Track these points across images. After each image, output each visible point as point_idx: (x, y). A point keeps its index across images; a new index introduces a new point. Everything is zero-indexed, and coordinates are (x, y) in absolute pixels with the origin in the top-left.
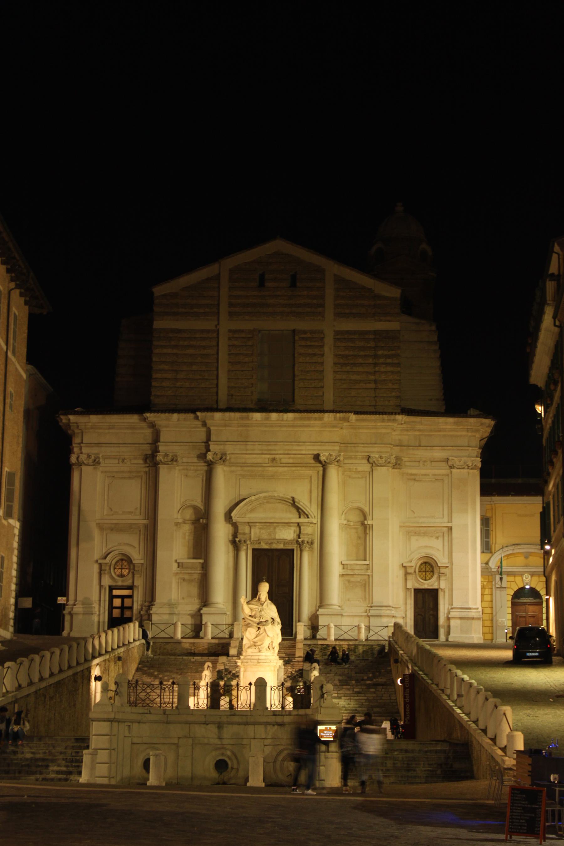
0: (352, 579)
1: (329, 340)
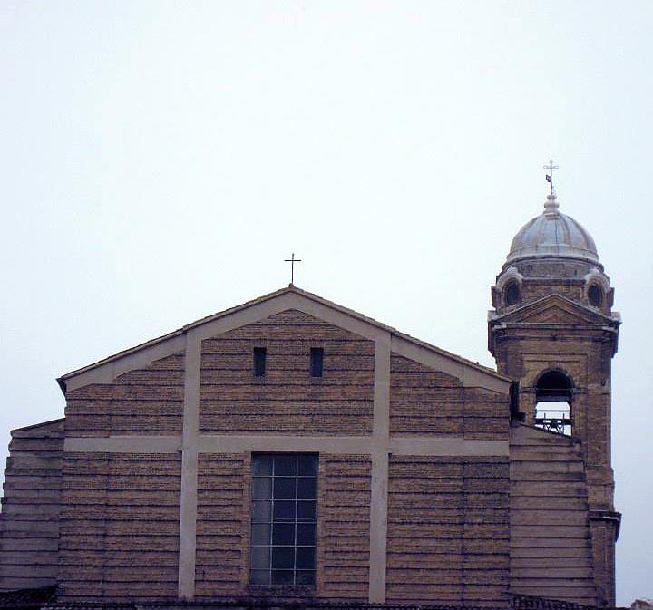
1: (380, 473)
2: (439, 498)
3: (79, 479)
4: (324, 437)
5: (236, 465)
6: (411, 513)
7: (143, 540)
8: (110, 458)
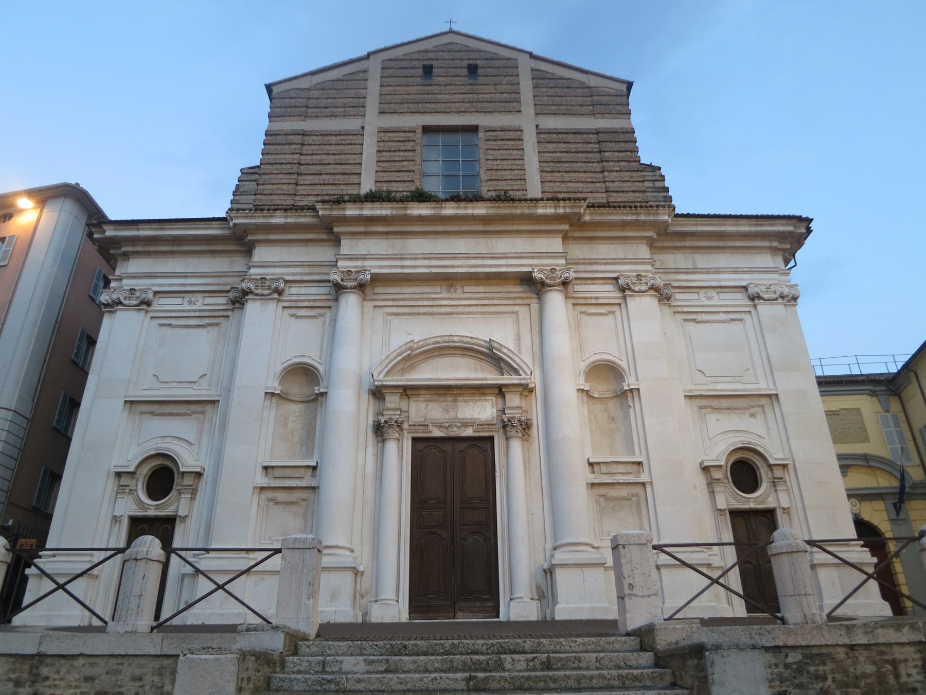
0: (612, 492)
2: (580, 155)
3: (278, 147)
4: (481, 116)
6: (559, 165)
7: (330, 187)
8: (304, 134)
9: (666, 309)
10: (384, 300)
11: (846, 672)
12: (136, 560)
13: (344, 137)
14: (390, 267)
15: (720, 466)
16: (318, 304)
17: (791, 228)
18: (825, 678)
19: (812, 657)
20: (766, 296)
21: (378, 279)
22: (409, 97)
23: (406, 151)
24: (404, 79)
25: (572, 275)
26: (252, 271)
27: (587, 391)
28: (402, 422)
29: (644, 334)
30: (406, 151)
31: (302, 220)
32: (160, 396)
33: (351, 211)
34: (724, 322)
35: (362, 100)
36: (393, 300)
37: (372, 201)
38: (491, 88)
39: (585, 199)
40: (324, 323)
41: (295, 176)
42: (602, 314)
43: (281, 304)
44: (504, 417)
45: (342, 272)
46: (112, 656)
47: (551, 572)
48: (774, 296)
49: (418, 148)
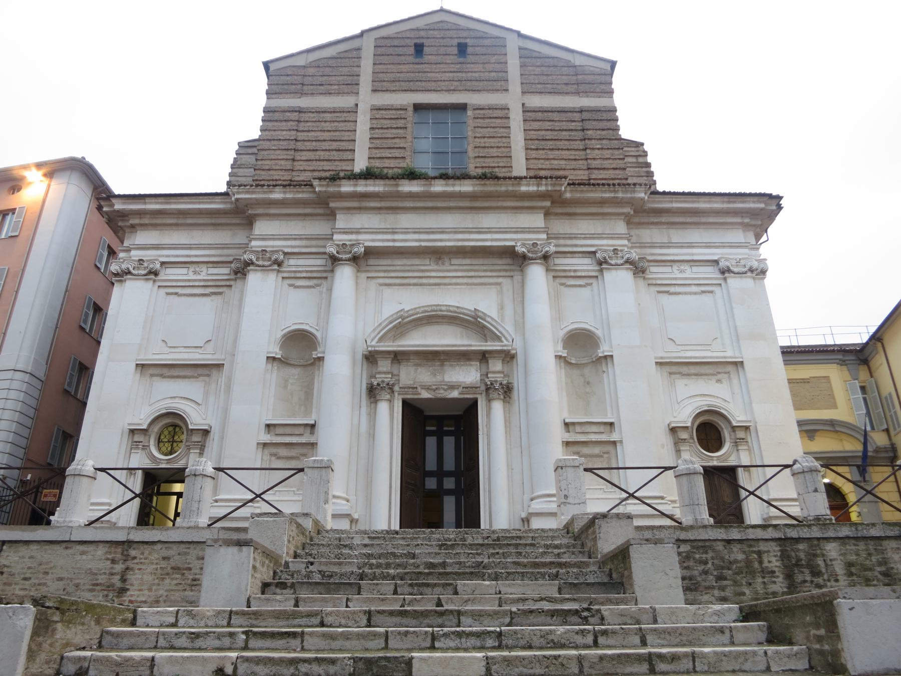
2: (564, 133)
3: (276, 124)
5: (401, 112)
7: (325, 163)
9: (641, 282)
10: (376, 271)
11: (722, 559)
12: (195, 475)
13: (338, 114)
14: (383, 240)
15: (687, 427)
16: (315, 275)
17: (762, 206)
18: (706, 563)
19: (698, 548)
20: (736, 270)
21: (370, 253)
22: (402, 75)
23: (397, 128)
24: (396, 57)
25: (552, 249)
26: (254, 243)
27: (565, 357)
28: (393, 385)
29: (618, 305)
30: (397, 128)
31: (300, 196)
32: (169, 360)
33: (347, 187)
34: (695, 293)
35: (356, 78)
36: (385, 271)
37: (366, 178)
38: (479, 67)
39: (565, 177)
40: (321, 293)
41: (292, 152)
42: (580, 286)
43: (281, 275)
44: (487, 380)
45: (338, 245)
46: (182, 542)
47: (528, 521)
48: (744, 270)
49: (409, 125)
